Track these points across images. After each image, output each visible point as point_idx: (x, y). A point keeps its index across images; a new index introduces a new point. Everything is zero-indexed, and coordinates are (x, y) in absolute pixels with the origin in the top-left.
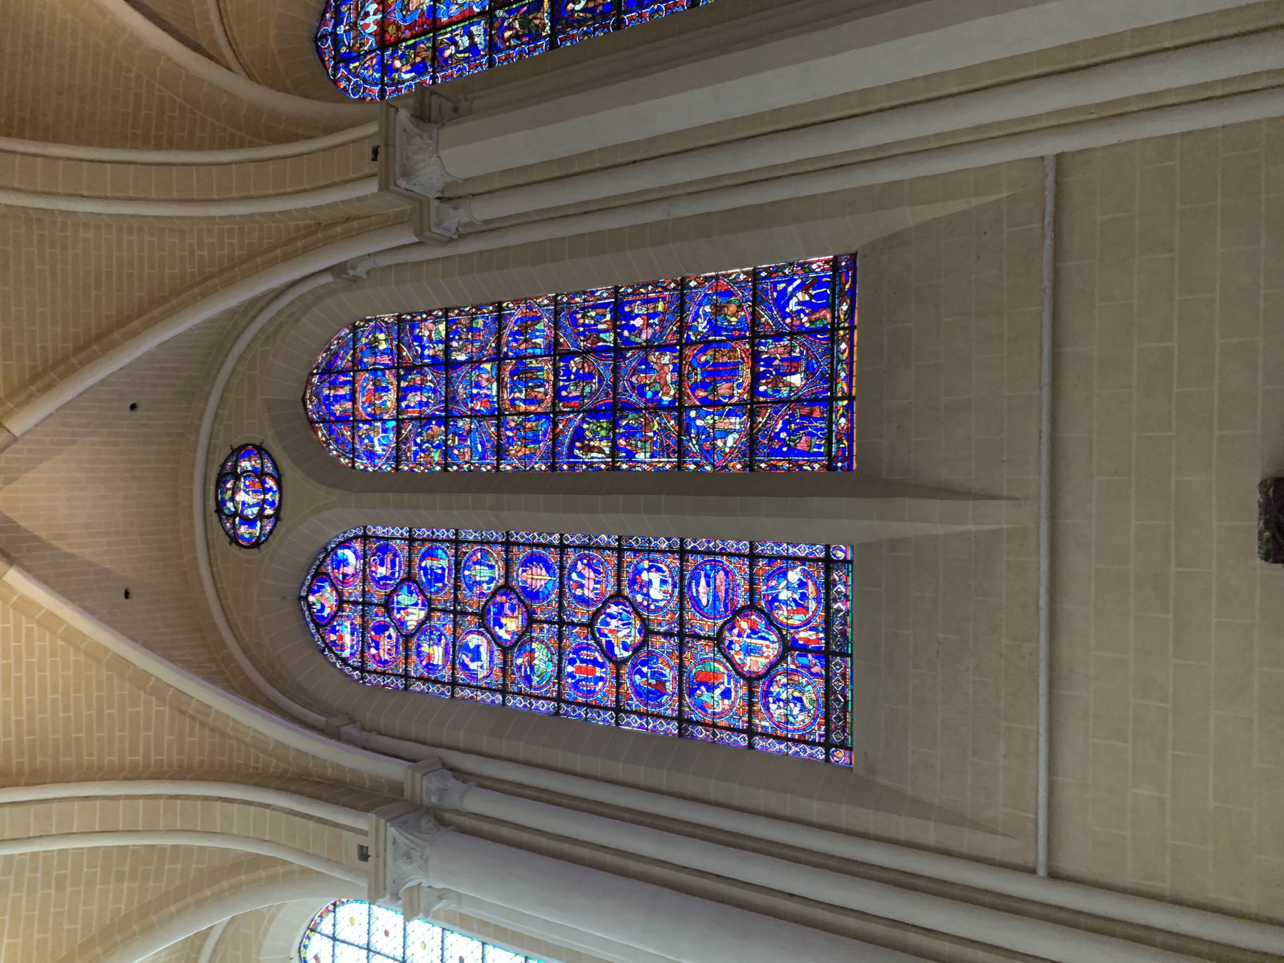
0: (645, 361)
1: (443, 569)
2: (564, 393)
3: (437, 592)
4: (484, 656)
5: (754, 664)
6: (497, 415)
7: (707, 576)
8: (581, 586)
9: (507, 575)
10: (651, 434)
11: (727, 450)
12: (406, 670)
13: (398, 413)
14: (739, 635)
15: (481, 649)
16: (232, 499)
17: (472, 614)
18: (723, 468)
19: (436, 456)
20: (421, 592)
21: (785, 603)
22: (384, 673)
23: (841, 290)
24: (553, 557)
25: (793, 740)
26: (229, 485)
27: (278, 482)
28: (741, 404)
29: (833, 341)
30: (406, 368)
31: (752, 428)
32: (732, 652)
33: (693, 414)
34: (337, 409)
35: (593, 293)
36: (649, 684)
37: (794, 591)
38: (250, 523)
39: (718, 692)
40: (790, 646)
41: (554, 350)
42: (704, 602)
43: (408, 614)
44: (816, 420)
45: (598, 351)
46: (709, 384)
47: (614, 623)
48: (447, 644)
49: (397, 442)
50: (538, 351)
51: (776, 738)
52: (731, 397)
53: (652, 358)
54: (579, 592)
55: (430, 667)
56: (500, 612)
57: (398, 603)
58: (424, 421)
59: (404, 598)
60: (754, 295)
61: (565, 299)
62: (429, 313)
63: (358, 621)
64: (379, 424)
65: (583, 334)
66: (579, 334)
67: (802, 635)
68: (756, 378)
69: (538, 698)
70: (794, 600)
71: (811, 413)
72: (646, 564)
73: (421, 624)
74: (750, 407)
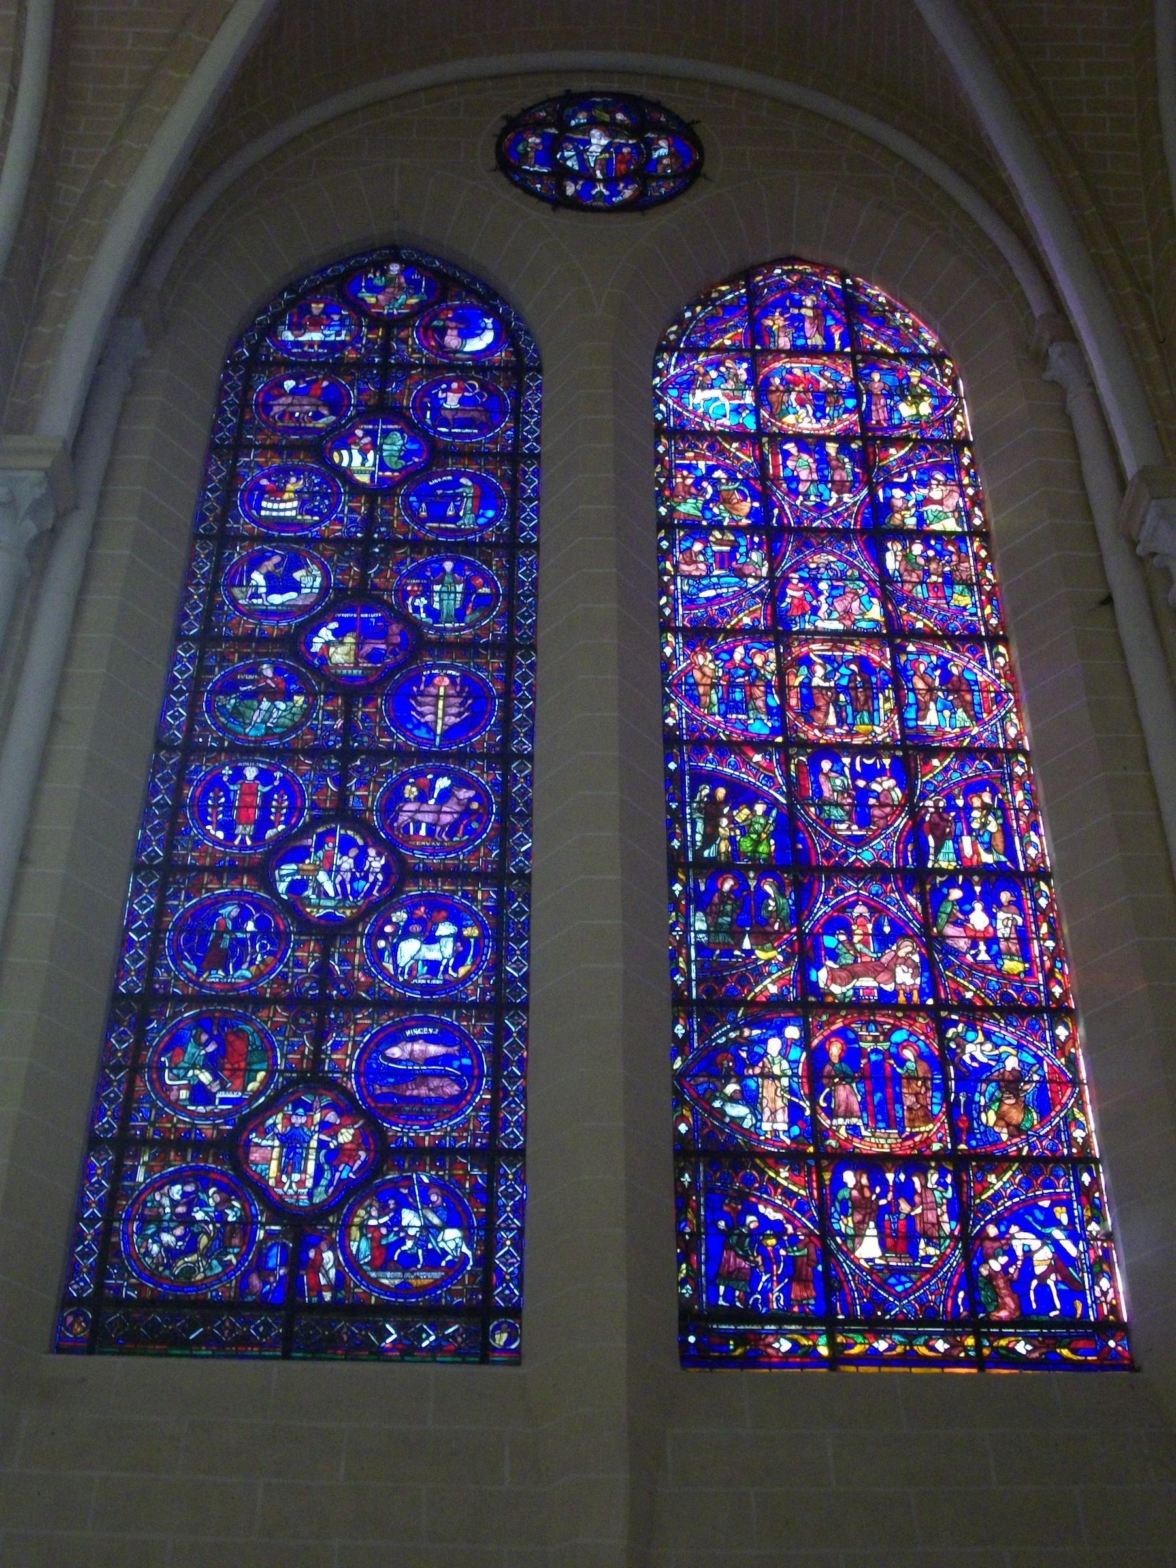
0: (900, 932)
1: (456, 518)
2: (826, 765)
3: (408, 506)
4: (276, 599)
5: (267, 1157)
6: (779, 629)
7: (446, 1059)
8: (422, 798)
9: (443, 647)
10: (747, 944)
12: (251, 445)
13: (772, 436)
14: (324, 1126)
15: (294, 595)
16: (593, 123)
17: (364, 576)
19: (689, 507)
20: (407, 474)
21: (396, 1220)
22: (245, 403)
23: (1059, 1341)
24: (480, 739)
25: (109, 1230)
26: (620, 116)
27: (626, 206)
28: (815, 1132)
29: (953, 1326)
30: (863, 451)
31: (765, 1155)
32: (289, 1109)
33: (792, 1032)
34: (776, 322)
35: (1035, 827)
36: (219, 935)
37: (421, 1242)
38: (547, 154)
39: (205, 1077)
40: (305, 1227)
41: (911, 751)
42: (395, 1052)
43: (363, 453)
44: (786, 1291)
45: (915, 835)
46: (855, 1066)
47: (347, 863)
48: (302, 526)
49: (713, 433)
50: (911, 714)
51: (113, 1195)
53: (905, 948)
54: (411, 791)
55: (255, 495)
56: (366, 632)
57: (386, 433)
58: (760, 486)
59: (395, 444)
60: (1042, 1158)
61: (1019, 770)
62: (976, 501)
63: (350, 355)
64: (749, 399)
65: (951, 806)
66: (950, 798)
67: (328, 1256)
68: (872, 1165)
69: (191, 706)
70: (402, 1242)
71: (803, 1282)
72: (471, 932)
73: (346, 475)
74: (813, 1153)
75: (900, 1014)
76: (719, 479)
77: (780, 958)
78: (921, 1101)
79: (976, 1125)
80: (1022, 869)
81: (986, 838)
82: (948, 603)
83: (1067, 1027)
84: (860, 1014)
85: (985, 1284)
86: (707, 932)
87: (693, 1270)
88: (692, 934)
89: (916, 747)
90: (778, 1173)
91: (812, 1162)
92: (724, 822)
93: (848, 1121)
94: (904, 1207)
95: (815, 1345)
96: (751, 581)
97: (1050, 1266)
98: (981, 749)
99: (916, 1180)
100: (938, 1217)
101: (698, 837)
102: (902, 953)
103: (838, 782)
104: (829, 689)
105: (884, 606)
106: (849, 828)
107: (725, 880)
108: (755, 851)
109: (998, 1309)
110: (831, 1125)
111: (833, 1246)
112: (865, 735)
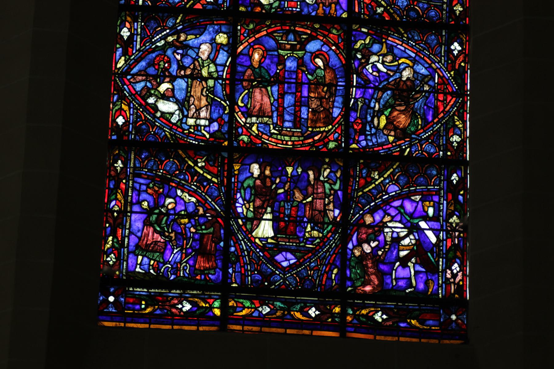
11: (151, 100)
18: (120, 92)
29: (325, 296)
33: (222, 39)
52: (248, 114)
68: (274, 159)
75: (317, 26)
79: (368, 128)
83: (461, 44)
85: (356, 263)
87: (118, 242)
90: (196, 163)
91: (225, 155)
93: (260, 119)
94: (298, 196)
95: (211, 308)
97: (412, 250)
99: (311, 173)
100: (325, 205)
109: (364, 284)
110: (246, 123)
111: (235, 227)
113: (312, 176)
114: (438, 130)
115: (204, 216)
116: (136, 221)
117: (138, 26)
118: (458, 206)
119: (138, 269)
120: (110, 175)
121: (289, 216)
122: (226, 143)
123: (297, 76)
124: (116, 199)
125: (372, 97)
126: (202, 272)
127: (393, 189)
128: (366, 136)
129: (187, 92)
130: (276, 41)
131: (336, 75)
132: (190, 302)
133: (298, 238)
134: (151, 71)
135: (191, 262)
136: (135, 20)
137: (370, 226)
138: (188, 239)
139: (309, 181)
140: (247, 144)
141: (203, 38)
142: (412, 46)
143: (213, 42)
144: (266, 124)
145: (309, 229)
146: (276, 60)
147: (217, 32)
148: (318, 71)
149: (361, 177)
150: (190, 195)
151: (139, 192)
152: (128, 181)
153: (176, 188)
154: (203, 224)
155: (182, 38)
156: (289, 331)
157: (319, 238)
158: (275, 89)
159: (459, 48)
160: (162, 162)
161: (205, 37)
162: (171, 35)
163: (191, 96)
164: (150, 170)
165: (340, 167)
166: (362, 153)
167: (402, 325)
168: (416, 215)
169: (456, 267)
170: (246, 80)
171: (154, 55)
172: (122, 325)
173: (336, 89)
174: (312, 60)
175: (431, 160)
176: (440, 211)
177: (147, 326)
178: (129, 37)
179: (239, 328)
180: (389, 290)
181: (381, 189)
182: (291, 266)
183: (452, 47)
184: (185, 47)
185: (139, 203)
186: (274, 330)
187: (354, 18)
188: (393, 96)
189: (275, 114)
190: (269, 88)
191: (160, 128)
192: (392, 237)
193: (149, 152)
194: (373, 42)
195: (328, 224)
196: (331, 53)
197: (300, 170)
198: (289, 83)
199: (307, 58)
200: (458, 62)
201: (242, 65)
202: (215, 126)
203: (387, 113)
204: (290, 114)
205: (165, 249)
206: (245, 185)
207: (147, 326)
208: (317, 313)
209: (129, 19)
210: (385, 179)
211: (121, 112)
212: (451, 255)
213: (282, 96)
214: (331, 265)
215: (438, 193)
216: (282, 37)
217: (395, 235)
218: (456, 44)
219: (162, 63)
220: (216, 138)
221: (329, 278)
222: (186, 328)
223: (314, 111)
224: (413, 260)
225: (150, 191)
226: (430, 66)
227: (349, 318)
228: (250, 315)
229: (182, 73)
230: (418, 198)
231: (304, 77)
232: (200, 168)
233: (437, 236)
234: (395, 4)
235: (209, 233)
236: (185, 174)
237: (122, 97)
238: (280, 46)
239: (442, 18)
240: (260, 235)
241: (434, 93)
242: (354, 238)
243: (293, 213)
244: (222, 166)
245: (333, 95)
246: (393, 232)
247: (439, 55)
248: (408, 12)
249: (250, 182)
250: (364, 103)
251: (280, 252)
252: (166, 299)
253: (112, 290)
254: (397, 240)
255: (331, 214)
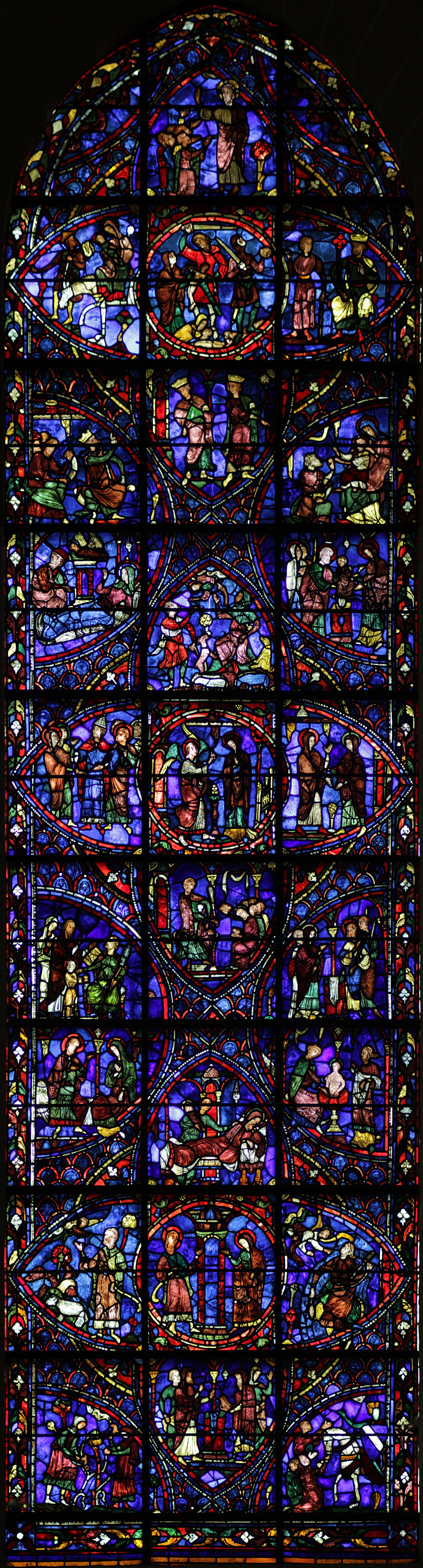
10: (89, 1121)
11: (51, 1302)
18: (15, 1293)
29: (258, 1519)
33: (130, 1221)
49: (84, 363)
52: (164, 1311)
75: (240, 1199)
76: (86, 446)
77: (123, 1135)
78: (252, 1294)
79: (303, 1320)
80: (390, 1017)
81: (356, 979)
82: (353, 642)
83: (409, 1212)
84: (201, 1199)
86: (49, 1106)
87: (23, 1471)
88: (33, 1109)
89: (291, 857)
90: (107, 1374)
91: (140, 1361)
92: (72, 966)
94: (225, 1405)
95: (132, 1539)
96: (119, 614)
97: (355, 1460)
98: (365, 858)
99: (238, 1377)
100: (256, 1414)
101: (43, 987)
102: (249, 1126)
103: (200, 907)
104: (199, 777)
105: (276, 651)
106: (207, 971)
107: (69, 1040)
108: (104, 1002)
109: (302, 1502)
110: (161, 1322)
111: (155, 1445)
112: (236, 841)
113: (240, 1381)
114: (384, 1318)
115: (118, 1435)
116: (43, 1445)
117: (31, 1212)
118: (407, 1406)
119: (48, 1501)
120: (10, 1394)
121: (215, 1429)
122: (140, 1348)
123: (219, 1262)
124: (18, 1421)
125: (307, 1282)
126: (120, 1499)
127: (333, 1390)
128: (301, 1329)
129: (92, 1289)
130: (194, 1220)
131: (264, 1258)
132: (108, 1535)
133: (227, 1453)
134: (49, 1266)
135: (107, 1489)
136: (27, 1205)
137: (307, 1435)
138: (102, 1462)
139: (237, 1387)
140: (164, 1347)
141: (107, 1222)
142: (352, 1217)
143: (119, 1225)
144: (185, 1322)
145: (238, 1443)
146: (193, 1243)
147: (124, 1214)
148: (243, 1254)
149: (296, 1378)
150: (102, 1412)
151: (44, 1412)
152: (30, 1400)
153: (86, 1404)
154: (119, 1444)
155: (83, 1224)
156: (219, 1560)
157: (250, 1452)
158: (194, 1279)
159: (407, 1216)
160: (68, 1374)
161: (110, 1221)
162: (70, 1221)
163: (97, 1293)
164: (55, 1385)
165: (271, 1368)
166: (298, 1350)
167: (345, 1545)
168: (360, 1418)
169: (405, 1476)
170: (159, 1271)
171: (51, 1247)
172: (34, 1564)
173: (265, 1275)
174: (236, 1242)
175: (375, 1354)
176: (386, 1412)
177: (61, 1564)
178: (21, 1226)
179: (164, 1560)
180: (330, 1507)
181: (319, 1391)
182: (220, 1487)
183: (399, 1215)
184: (87, 1234)
185: (45, 1424)
186: (203, 1560)
187: (284, 1185)
188: (331, 1279)
189: (195, 1310)
190: (187, 1279)
191: (64, 1335)
192: (332, 1446)
193: (52, 1364)
194: (307, 1215)
195: (260, 1436)
196: (257, 1230)
197: (226, 1375)
198: (209, 1271)
199: (230, 1239)
200: (406, 1233)
201: (154, 1253)
202: (127, 1328)
203: (324, 1300)
204: (212, 1309)
205: (77, 1475)
206: (164, 1396)
207: (61, 1564)
208: (251, 1537)
209: (19, 1203)
210: (323, 1379)
211: (17, 1318)
212: (399, 1463)
213: (202, 1287)
214: (265, 1482)
215: (384, 1391)
216: (199, 1215)
217: (336, 1444)
218: (403, 1211)
219: (61, 1256)
220: (128, 1343)
221: (263, 1498)
222: (105, 1563)
223: (241, 1303)
224: (357, 1471)
225: (56, 1410)
226: (374, 1241)
227: (286, 1542)
228: (175, 1545)
229: (86, 1266)
230: (361, 1399)
231: (227, 1262)
232: (112, 1379)
233: (384, 1442)
234: (331, 1165)
235: (126, 1454)
236: (95, 1387)
237: (17, 1300)
238: (198, 1227)
239: (387, 1179)
240: (183, 1453)
241: (379, 1272)
242: (290, 1450)
243: (220, 1425)
244: (137, 1374)
245: (261, 1282)
246: (334, 1440)
247: (383, 1226)
248: (347, 1173)
249: (169, 1392)
250: (298, 1290)
251: (207, 1472)
252: (81, 1532)
253: (20, 1526)
254: (338, 1449)
255: (263, 1424)
